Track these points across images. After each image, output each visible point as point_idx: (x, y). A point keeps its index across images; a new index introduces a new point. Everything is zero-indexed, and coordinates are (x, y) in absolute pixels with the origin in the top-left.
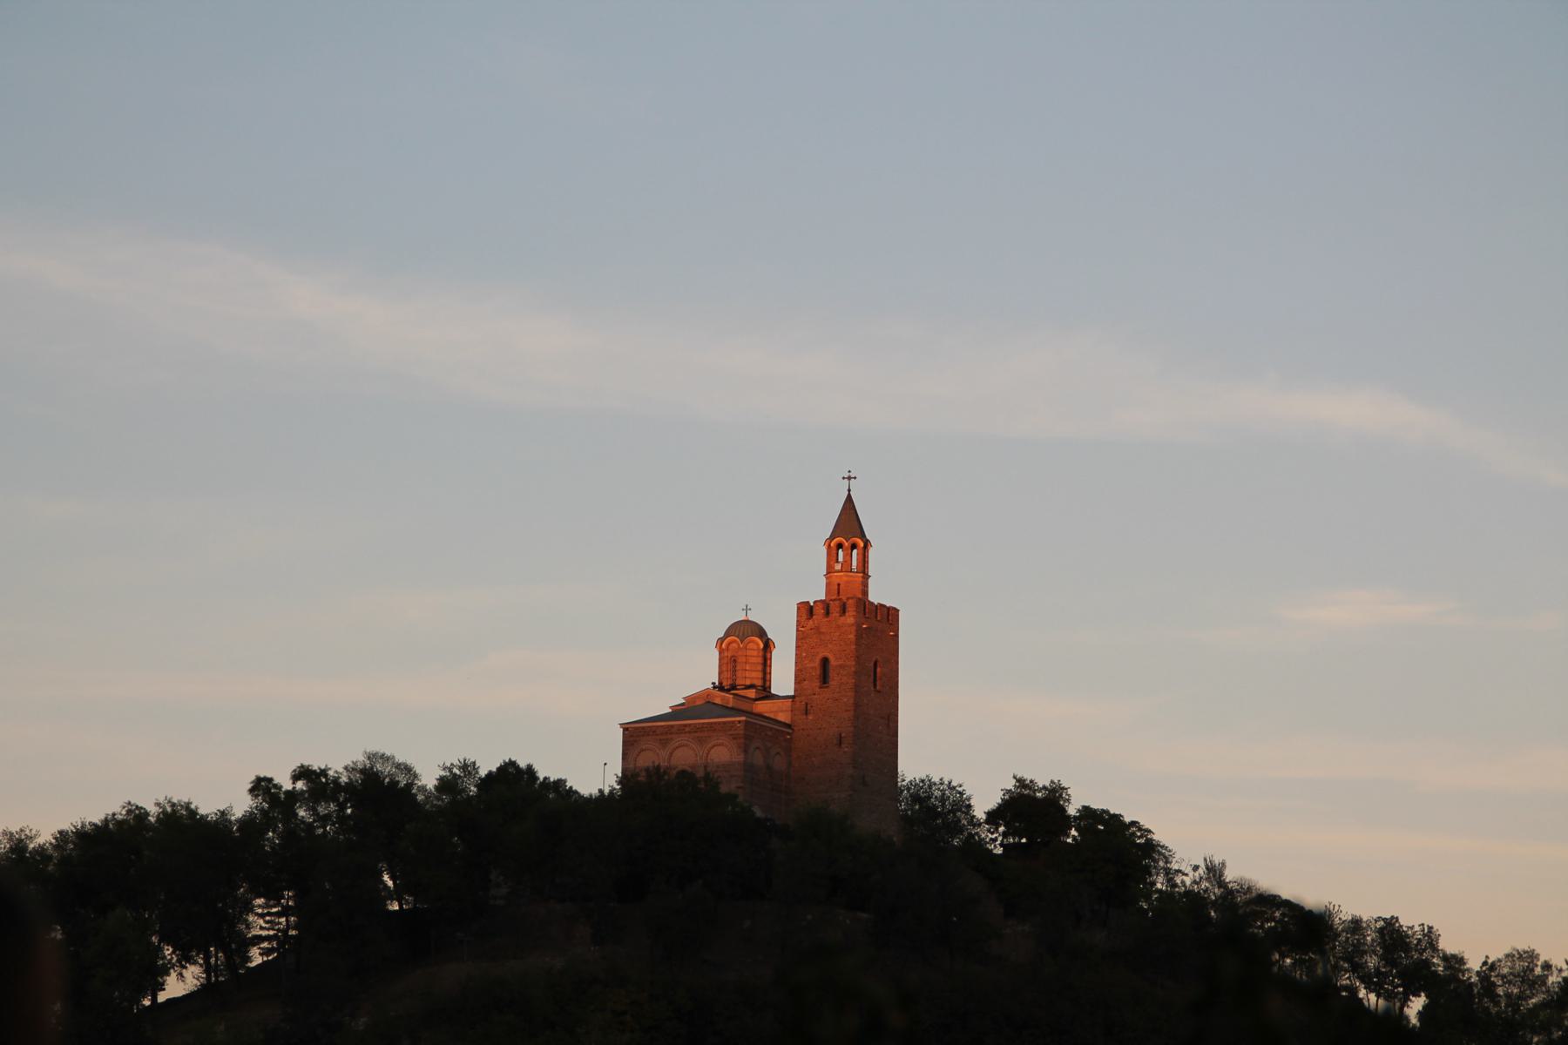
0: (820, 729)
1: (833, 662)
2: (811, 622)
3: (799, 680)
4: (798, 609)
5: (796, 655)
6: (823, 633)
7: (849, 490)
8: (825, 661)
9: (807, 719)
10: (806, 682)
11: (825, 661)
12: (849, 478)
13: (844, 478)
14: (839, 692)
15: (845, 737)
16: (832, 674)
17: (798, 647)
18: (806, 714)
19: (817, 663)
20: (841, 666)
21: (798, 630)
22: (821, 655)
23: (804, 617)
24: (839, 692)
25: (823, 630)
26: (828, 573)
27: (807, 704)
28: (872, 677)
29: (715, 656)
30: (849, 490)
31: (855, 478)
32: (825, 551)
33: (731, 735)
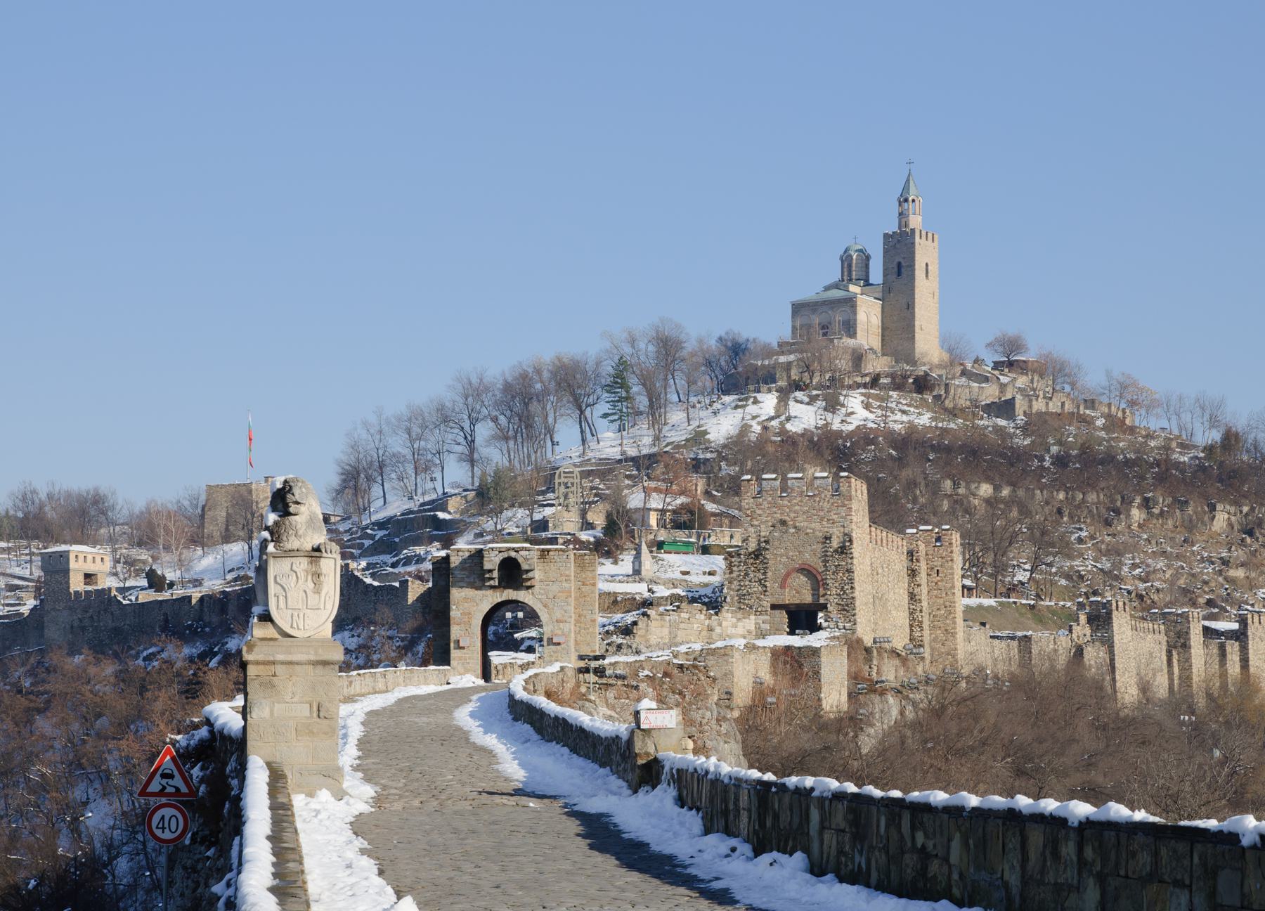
1: (903, 264)
3: (885, 275)
8: (899, 264)
11: (899, 264)
16: (903, 270)
19: (895, 263)
20: (908, 266)
22: (897, 260)
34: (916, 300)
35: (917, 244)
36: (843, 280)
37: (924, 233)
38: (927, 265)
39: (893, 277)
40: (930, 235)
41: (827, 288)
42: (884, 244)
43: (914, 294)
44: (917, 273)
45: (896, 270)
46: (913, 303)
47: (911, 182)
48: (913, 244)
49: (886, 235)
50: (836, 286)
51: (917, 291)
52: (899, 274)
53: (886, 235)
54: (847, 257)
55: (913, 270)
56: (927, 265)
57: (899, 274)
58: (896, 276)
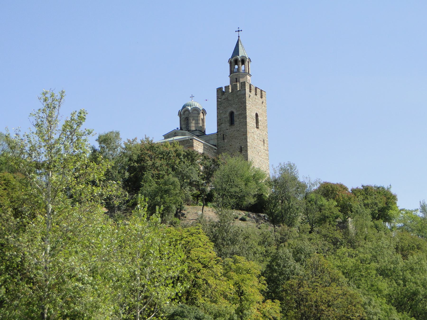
0: (231, 145)
1: (236, 113)
2: (224, 96)
3: (219, 124)
4: (217, 91)
5: (217, 112)
6: (230, 100)
7: (239, 37)
8: (232, 114)
9: (224, 142)
10: (222, 125)
11: (232, 114)
12: (239, 31)
13: (236, 31)
14: (239, 127)
15: (243, 148)
16: (235, 119)
17: (218, 109)
18: (224, 140)
19: (228, 115)
20: (239, 114)
21: (217, 101)
22: (229, 111)
23: (220, 94)
24: (239, 127)
25: (230, 99)
26: (231, 73)
27: (224, 135)
28: (255, 120)
29: (178, 118)
30: (239, 37)
31: (241, 31)
32: (229, 65)
33: (187, 146)
34: (248, 144)
35: (247, 96)
36: (181, 129)
37: (253, 88)
38: (257, 115)
39: (227, 125)
40: (258, 91)
41: (167, 136)
42: (218, 98)
43: (246, 139)
44: (248, 120)
45: (229, 119)
46: (246, 146)
47: (240, 46)
48: (245, 94)
49: (219, 90)
50: (174, 134)
51: (249, 135)
52: (232, 122)
53: (219, 90)
54: (184, 112)
55: (245, 118)
56: (257, 115)
57: (232, 122)
58: (228, 124)
